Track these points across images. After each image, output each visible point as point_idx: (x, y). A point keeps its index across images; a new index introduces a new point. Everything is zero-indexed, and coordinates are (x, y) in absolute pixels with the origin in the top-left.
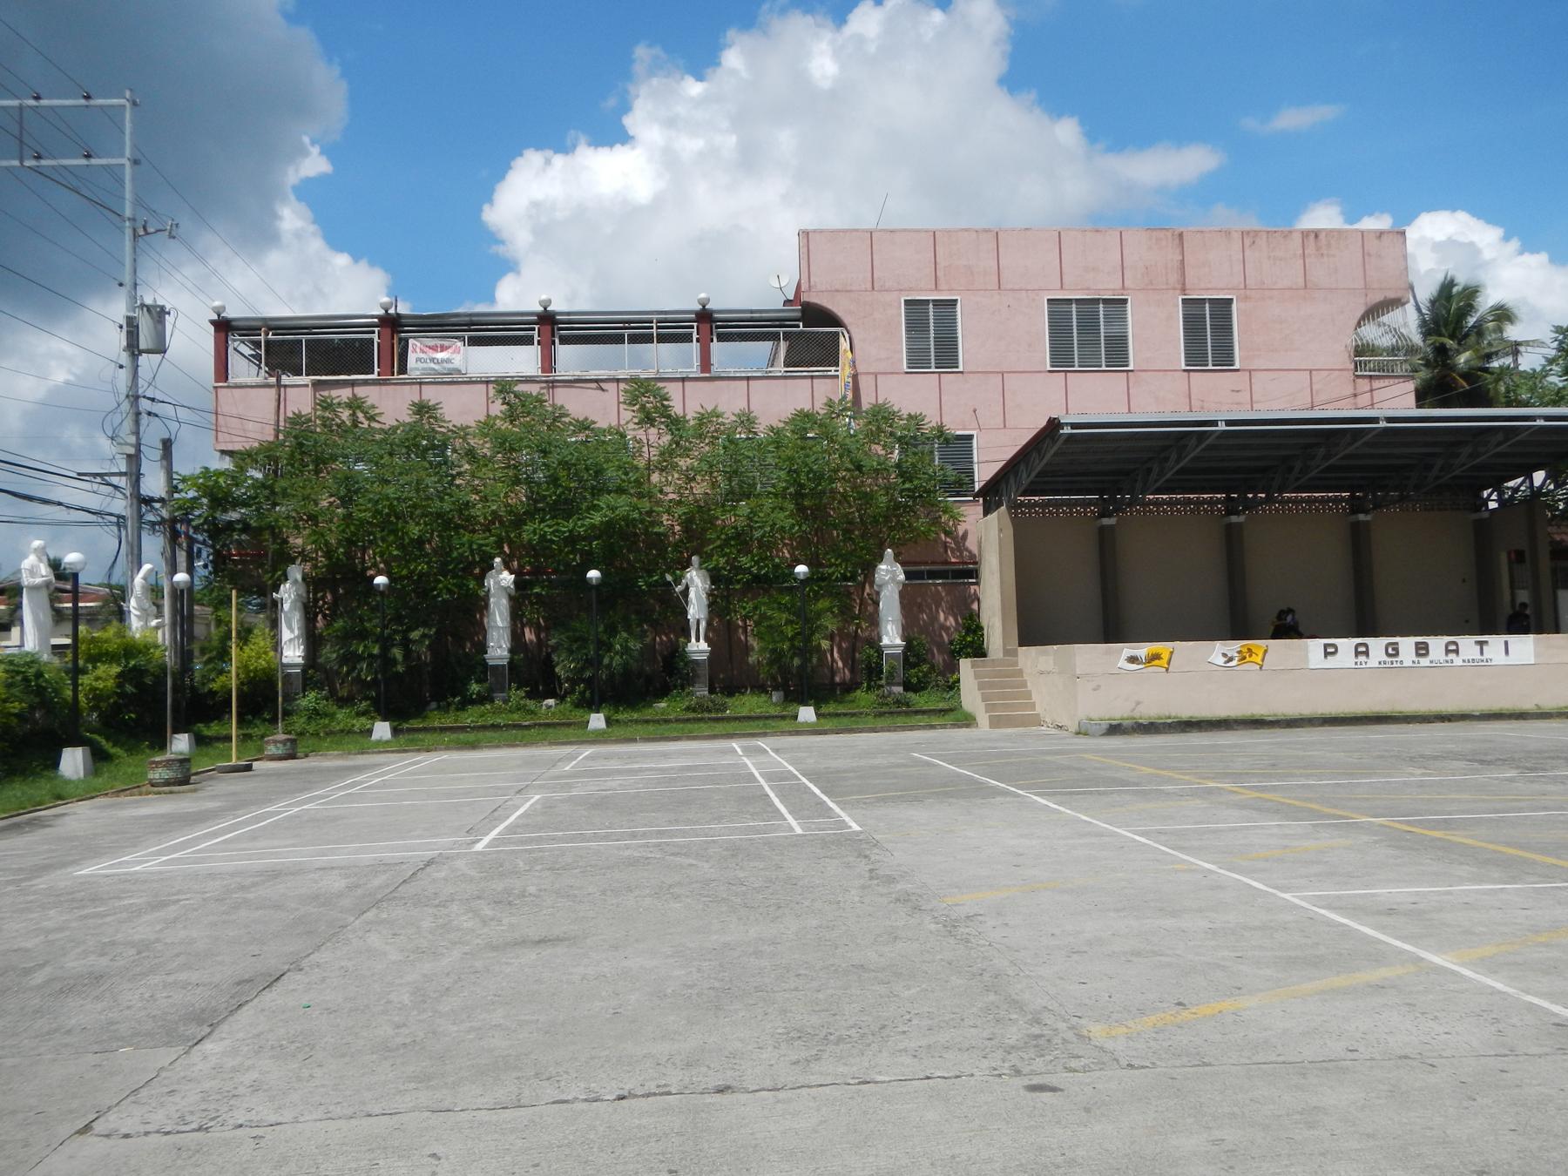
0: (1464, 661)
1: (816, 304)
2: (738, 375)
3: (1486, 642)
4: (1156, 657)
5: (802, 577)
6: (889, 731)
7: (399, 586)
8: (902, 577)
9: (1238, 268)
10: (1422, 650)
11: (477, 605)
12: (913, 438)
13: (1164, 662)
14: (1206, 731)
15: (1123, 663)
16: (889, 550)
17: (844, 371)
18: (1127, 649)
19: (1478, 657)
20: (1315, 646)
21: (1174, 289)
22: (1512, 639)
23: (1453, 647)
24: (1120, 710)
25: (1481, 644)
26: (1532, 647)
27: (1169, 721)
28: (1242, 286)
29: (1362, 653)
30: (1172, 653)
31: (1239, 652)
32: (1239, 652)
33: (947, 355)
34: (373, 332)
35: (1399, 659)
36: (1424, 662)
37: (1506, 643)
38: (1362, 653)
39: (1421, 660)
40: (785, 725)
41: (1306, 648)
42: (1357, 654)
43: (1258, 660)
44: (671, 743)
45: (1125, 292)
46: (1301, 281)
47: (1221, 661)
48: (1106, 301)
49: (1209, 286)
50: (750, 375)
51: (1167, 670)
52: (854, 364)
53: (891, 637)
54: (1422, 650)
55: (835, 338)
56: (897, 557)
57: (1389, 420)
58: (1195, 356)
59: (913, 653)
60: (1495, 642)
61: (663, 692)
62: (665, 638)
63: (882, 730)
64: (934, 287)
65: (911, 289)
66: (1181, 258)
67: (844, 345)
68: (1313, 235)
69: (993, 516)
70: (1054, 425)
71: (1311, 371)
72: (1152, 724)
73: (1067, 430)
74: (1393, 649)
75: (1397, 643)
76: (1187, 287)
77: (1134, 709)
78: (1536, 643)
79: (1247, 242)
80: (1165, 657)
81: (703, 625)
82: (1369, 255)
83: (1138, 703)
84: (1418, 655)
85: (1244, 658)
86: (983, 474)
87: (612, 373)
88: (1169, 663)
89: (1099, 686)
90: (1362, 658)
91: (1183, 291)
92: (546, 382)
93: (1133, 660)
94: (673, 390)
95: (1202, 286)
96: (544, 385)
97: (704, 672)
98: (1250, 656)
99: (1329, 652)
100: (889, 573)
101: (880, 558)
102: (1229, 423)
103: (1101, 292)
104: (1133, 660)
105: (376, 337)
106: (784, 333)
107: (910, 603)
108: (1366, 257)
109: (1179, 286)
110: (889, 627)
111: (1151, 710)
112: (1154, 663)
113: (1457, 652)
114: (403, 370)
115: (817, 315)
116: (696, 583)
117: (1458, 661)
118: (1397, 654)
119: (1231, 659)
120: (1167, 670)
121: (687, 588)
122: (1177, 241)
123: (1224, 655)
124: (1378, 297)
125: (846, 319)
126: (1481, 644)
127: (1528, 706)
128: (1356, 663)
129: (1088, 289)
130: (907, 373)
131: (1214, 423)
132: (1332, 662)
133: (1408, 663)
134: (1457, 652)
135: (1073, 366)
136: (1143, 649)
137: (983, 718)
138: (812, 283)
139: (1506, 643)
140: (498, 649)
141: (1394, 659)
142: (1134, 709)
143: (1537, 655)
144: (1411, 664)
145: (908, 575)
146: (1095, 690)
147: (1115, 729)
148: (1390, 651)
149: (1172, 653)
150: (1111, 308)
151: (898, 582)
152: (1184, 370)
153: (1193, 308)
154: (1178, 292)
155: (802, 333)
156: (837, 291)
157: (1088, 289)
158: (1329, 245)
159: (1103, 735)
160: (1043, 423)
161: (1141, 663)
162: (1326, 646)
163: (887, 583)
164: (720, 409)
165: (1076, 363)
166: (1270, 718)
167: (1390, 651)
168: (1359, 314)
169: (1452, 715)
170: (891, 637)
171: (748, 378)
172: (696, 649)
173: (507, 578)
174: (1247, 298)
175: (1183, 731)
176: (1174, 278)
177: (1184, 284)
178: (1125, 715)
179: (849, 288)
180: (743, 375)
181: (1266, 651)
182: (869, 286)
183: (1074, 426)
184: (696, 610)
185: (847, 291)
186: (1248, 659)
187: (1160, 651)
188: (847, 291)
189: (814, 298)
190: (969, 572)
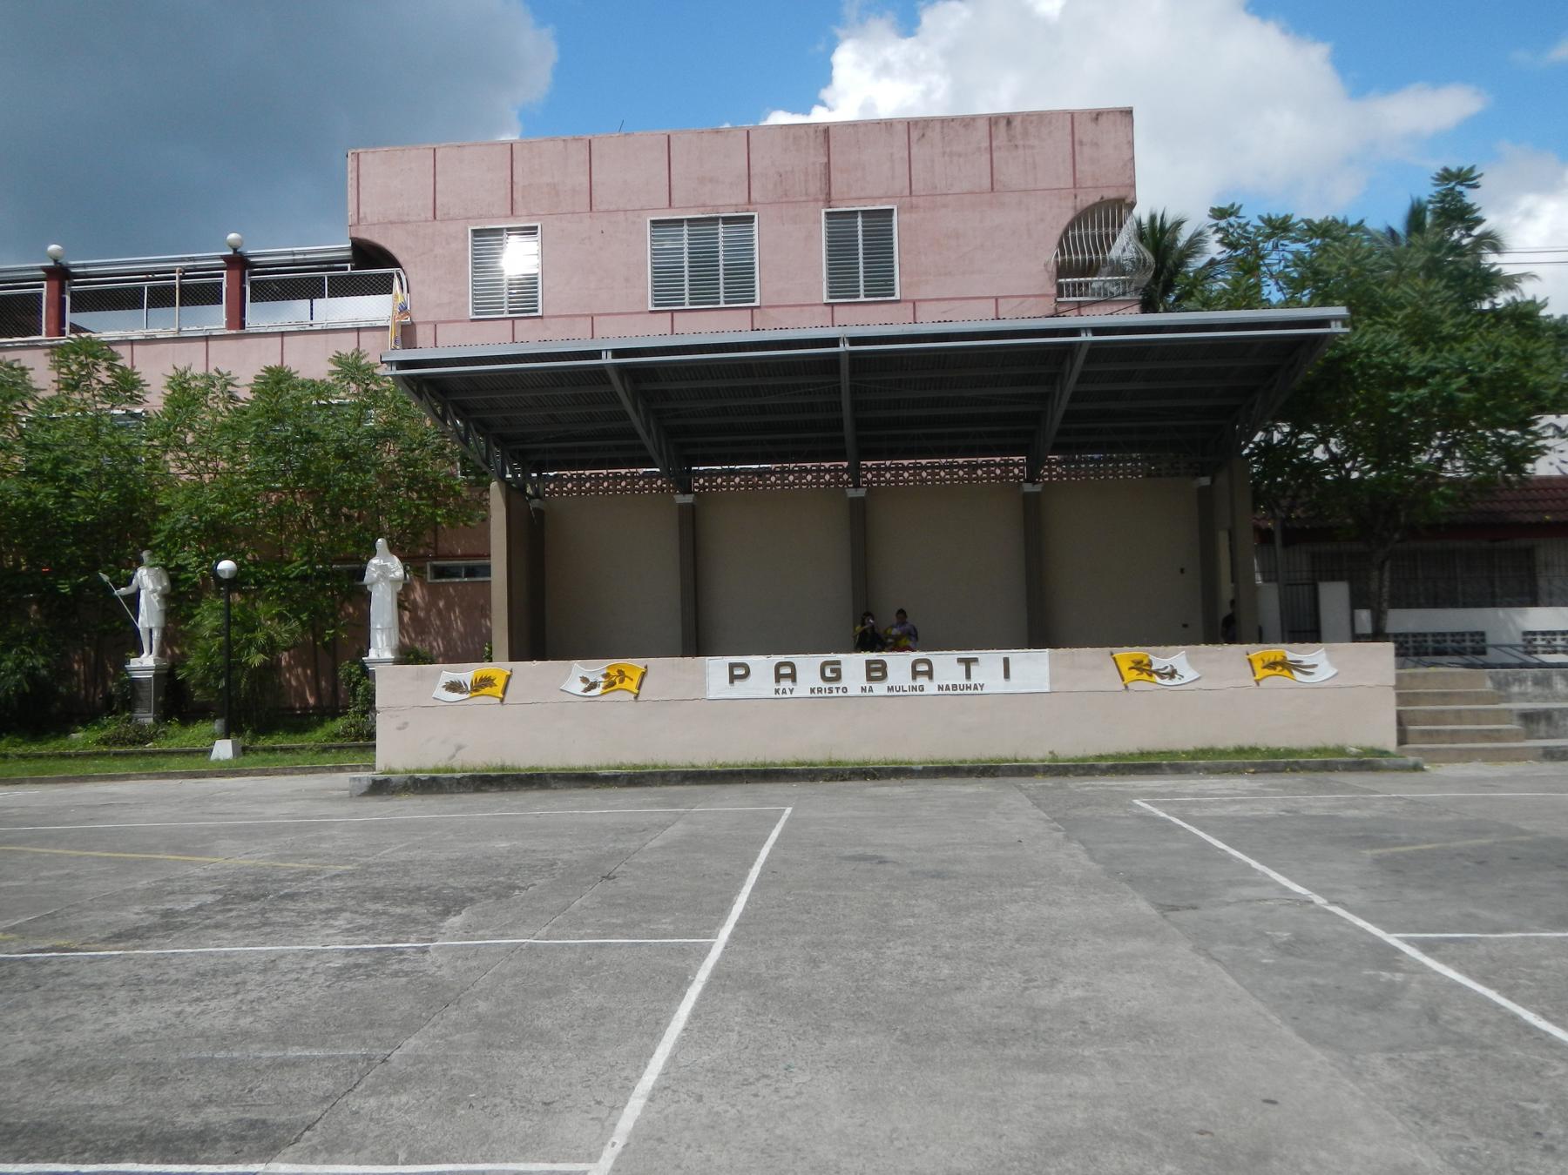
0: (940, 688)
1: (366, 241)
2: (269, 330)
3: (975, 660)
4: (484, 683)
5: (226, 576)
6: (285, 774)
7: (65, 589)
8: (399, 573)
9: (902, 169)
10: (876, 672)
13: (497, 690)
14: (510, 790)
16: (379, 540)
18: (449, 673)
19: (962, 681)
20: (716, 667)
21: (816, 200)
22: (1016, 656)
23: (924, 668)
25: (968, 662)
26: (1047, 668)
27: (458, 775)
28: (907, 192)
29: (786, 676)
30: (509, 677)
31: (606, 676)
32: (606, 676)
35: (841, 685)
36: (880, 689)
37: (1006, 661)
38: (786, 676)
39: (875, 685)
40: (193, 764)
41: (703, 673)
42: (779, 677)
43: (633, 686)
44: (102, 784)
45: (751, 207)
46: (986, 183)
47: (578, 687)
48: (727, 220)
49: (863, 194)
50: (283, 329)
51: (502, 700)
54: (876, 672)
56: (392, 549)
57: (854, 341)
60: (989, 662)
61: (88, 717)
62: (177, 651)
63: (276, 773)
64: (510, 212)
65: (480, 217)
66: (826, 160)
68: (1003, 123)
71: (996, 299)
72: (434, 779)
74: (833, 671)
75: (838, 663)
76: (833, 195)
77: (454, 756)
78: (1052, 662)
79: (915, 135)
81: (155, 634)
82: (1081, 143)
83: (459, 748)
84: (870, 679)
85: (613, 684)
87: (122, 333)
88: (504, 692)
89: (406, 724)
90: (786, 684)
91: (828, 201)
92: (51, 347)
93: (454, 687)
94: (123, 351)
95: (853, 195)
96: (48, 351)
97: (150, 696)
98: (622, 681)
99: (737, 675)
101: (372, 552)
103: (721, 209)
104: (454, 687)
106: (329, 278)
108: (1077, 147)
109: (823, 197)
110: (378, 638)
112: (483, 691)
113: (930, 674)
116: (148, 582)
117: (931, 688)
118: (838, 678)
119: (593, 686)
120: (502, 700)
121: (139, 590)
122: (821, 139)
123: (584, 680)
124: (1094, 198)
125: (401, 260)
126: (968, 662)
127: (1037, 753)
128: (777, 691)
129: (704, 206)
130: (473, 320)
132: (741, 689)
133: (854, 691)
135: (683, 304)
138: (361, 215)
139: (1006, 661)
141: (834, 685)
142: (454, 756)
143: (1053, 679)
144: (859, 693)
146: (399, 729)
148: (828, 673)
149: (509, 677)
150: (735, 229)
151: (394, 581)
152: (826, 304)
154: (821, 204)
155: (351, 277)
156: (391, 223)
157: (704, 206)
158: (1026, 134)
159: (364, 794)
161: (466, 691)
162: (732, 666)
163: (377, 581)
164: (181, 368)
165: (687, 301)
166: (605, 772)
167: (828, 673)
168: (1065, 221)
169: (879, 770)
171: (282, 334)
172: (139, 665)
174: (912, 208)
175: (478, 790)
176: (815, 186)
177: (829, 194)
178: (441, 765)
179: (406, 218)
180: (276, 330)
181: (644, 675)
182: (431, 214)
184: (149, 617)
185: (403, 222)
186: (618, 685)
187: (493, 675)
188: (403, 222)
189: (365, 235)
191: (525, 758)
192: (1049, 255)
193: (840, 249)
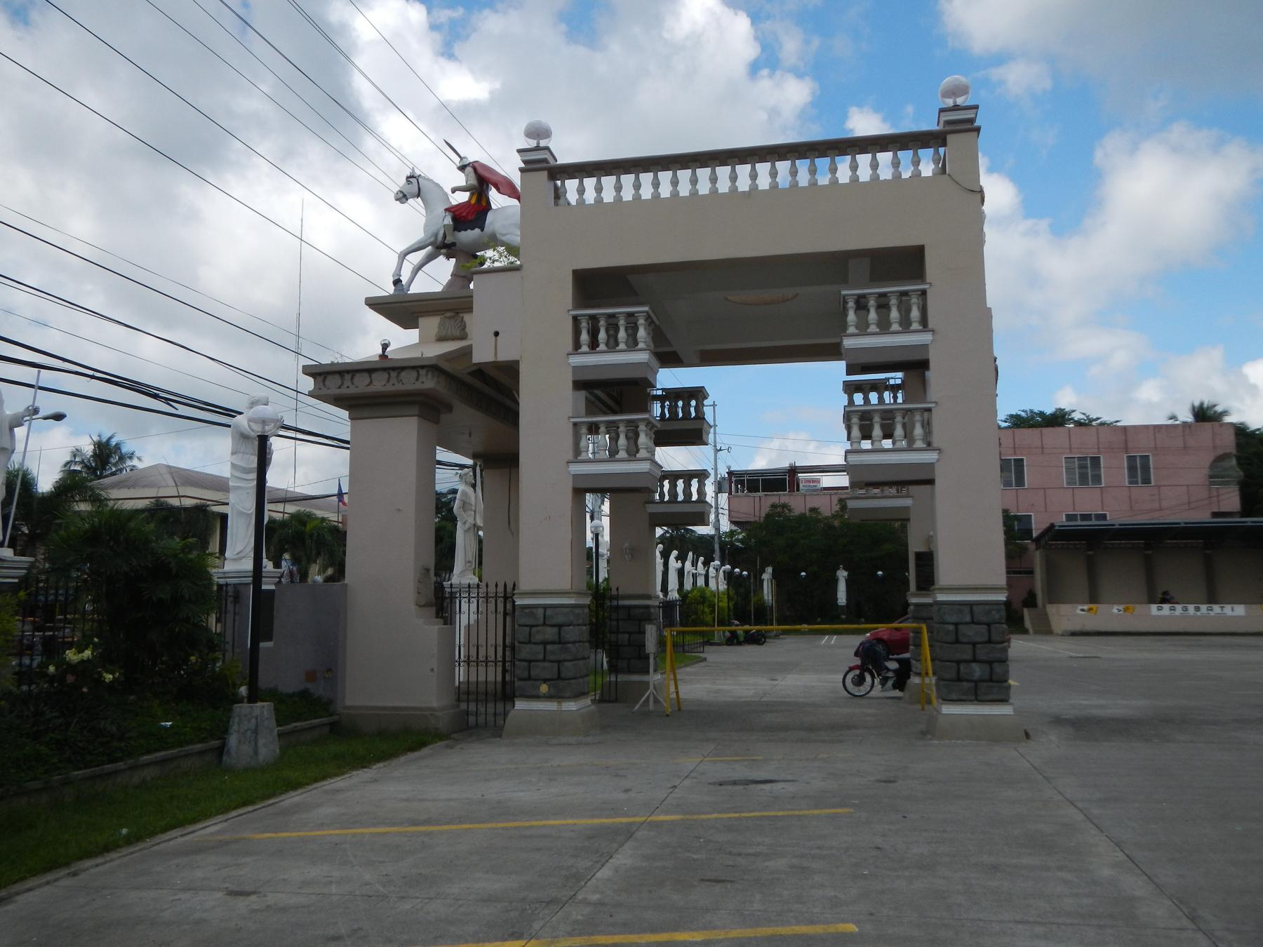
11: (836, 581)
15: (1079, 612)
20: (1154, 607)
22: (1235, 606)
24: (1077, 628)
25: (1222, 607)
33: (1020, 481)
34: (786, 475)
36: (1198, 613)
41: (1150, 609)
54: (1197, 609)
58: (1133, 481)
66: (1124, 438)
69: (1038, 552)
70: (1052, 525)
73: (1057, 528)
80: (1095, 609)
86: (1035, 535)
91: (1126, 450)
93: (1083, 610)
102: (1120, 525)
104: (1083, 610)
105: (787, 477)
111: (1089, 628)
114: (798, 490)
118: (1187, 610)
124: (1220, 452)
126: (1222, 607)
131: (1113, 525)
134: (1211, 610)
136: (1086, 607)
137: (1031, 631)
140: (842, 597)
147: (1074, 634)
153: (1132, 459)
160: (1048, 525)
173: (845, 574)
183: (1060, 526)
190: (1031, 572)
191: (1103, 629)
192: (1206, 471)
193: (1132, 469)
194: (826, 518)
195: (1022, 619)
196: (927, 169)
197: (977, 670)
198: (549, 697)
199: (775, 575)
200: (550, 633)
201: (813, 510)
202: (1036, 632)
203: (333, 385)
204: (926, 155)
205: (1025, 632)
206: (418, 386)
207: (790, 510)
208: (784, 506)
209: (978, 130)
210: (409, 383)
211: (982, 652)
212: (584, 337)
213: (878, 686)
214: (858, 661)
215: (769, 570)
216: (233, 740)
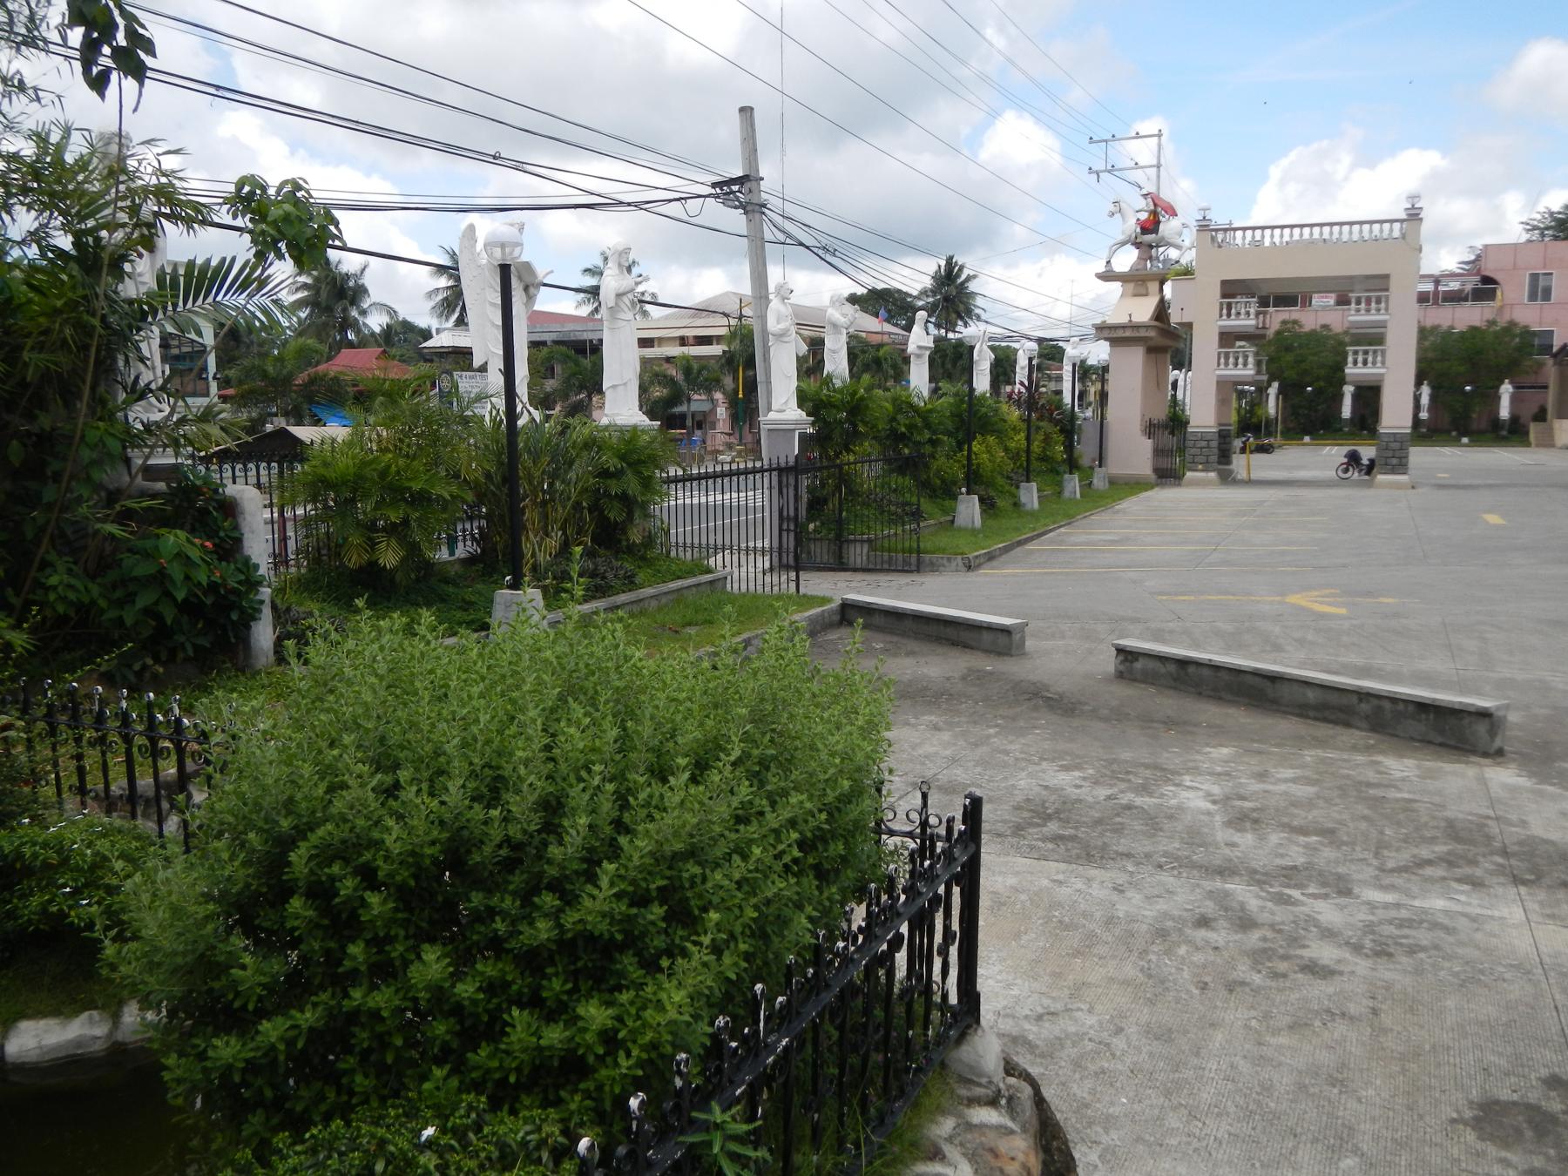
11: (1341, 396)
12: (1527, 333)
17: (1497, 303)
52: (1503, 300)
53: (1504, 413)
55: (1495, 289)
59: (1515, 419)
67: (1499, 293)
100: (1506, 389)
101: (1502, 383)
107: (1514, 399)
115: (1487, 280)
140: (1346, 411)
145: (1516, 387)
170: (1504, 413)
190: (1546, 387)
194: (1337, 334)
195: (1527, 433)
196: (1396, 234)
197: (1395, 461)
198: (1202, 471)
199: (1280, 391)
200: (1204, 444)
201: (1325, 327)
202: (1538, 446)
203: (1106, 333)
204: (1397, 226)
205: (1528, 444)
206: (1147, 334)
207: (1301, 326)
208: (1295, 322)
209: (1421, 219)
210: (1143, 333)
211: (1398, 454)
212: (1225, 311)
213: (1356, 474)
214: (1346, 460)
215: (1276, 385)
216: (1095, 481)
